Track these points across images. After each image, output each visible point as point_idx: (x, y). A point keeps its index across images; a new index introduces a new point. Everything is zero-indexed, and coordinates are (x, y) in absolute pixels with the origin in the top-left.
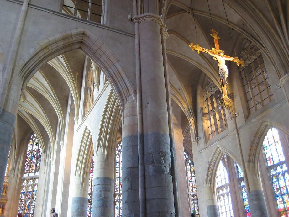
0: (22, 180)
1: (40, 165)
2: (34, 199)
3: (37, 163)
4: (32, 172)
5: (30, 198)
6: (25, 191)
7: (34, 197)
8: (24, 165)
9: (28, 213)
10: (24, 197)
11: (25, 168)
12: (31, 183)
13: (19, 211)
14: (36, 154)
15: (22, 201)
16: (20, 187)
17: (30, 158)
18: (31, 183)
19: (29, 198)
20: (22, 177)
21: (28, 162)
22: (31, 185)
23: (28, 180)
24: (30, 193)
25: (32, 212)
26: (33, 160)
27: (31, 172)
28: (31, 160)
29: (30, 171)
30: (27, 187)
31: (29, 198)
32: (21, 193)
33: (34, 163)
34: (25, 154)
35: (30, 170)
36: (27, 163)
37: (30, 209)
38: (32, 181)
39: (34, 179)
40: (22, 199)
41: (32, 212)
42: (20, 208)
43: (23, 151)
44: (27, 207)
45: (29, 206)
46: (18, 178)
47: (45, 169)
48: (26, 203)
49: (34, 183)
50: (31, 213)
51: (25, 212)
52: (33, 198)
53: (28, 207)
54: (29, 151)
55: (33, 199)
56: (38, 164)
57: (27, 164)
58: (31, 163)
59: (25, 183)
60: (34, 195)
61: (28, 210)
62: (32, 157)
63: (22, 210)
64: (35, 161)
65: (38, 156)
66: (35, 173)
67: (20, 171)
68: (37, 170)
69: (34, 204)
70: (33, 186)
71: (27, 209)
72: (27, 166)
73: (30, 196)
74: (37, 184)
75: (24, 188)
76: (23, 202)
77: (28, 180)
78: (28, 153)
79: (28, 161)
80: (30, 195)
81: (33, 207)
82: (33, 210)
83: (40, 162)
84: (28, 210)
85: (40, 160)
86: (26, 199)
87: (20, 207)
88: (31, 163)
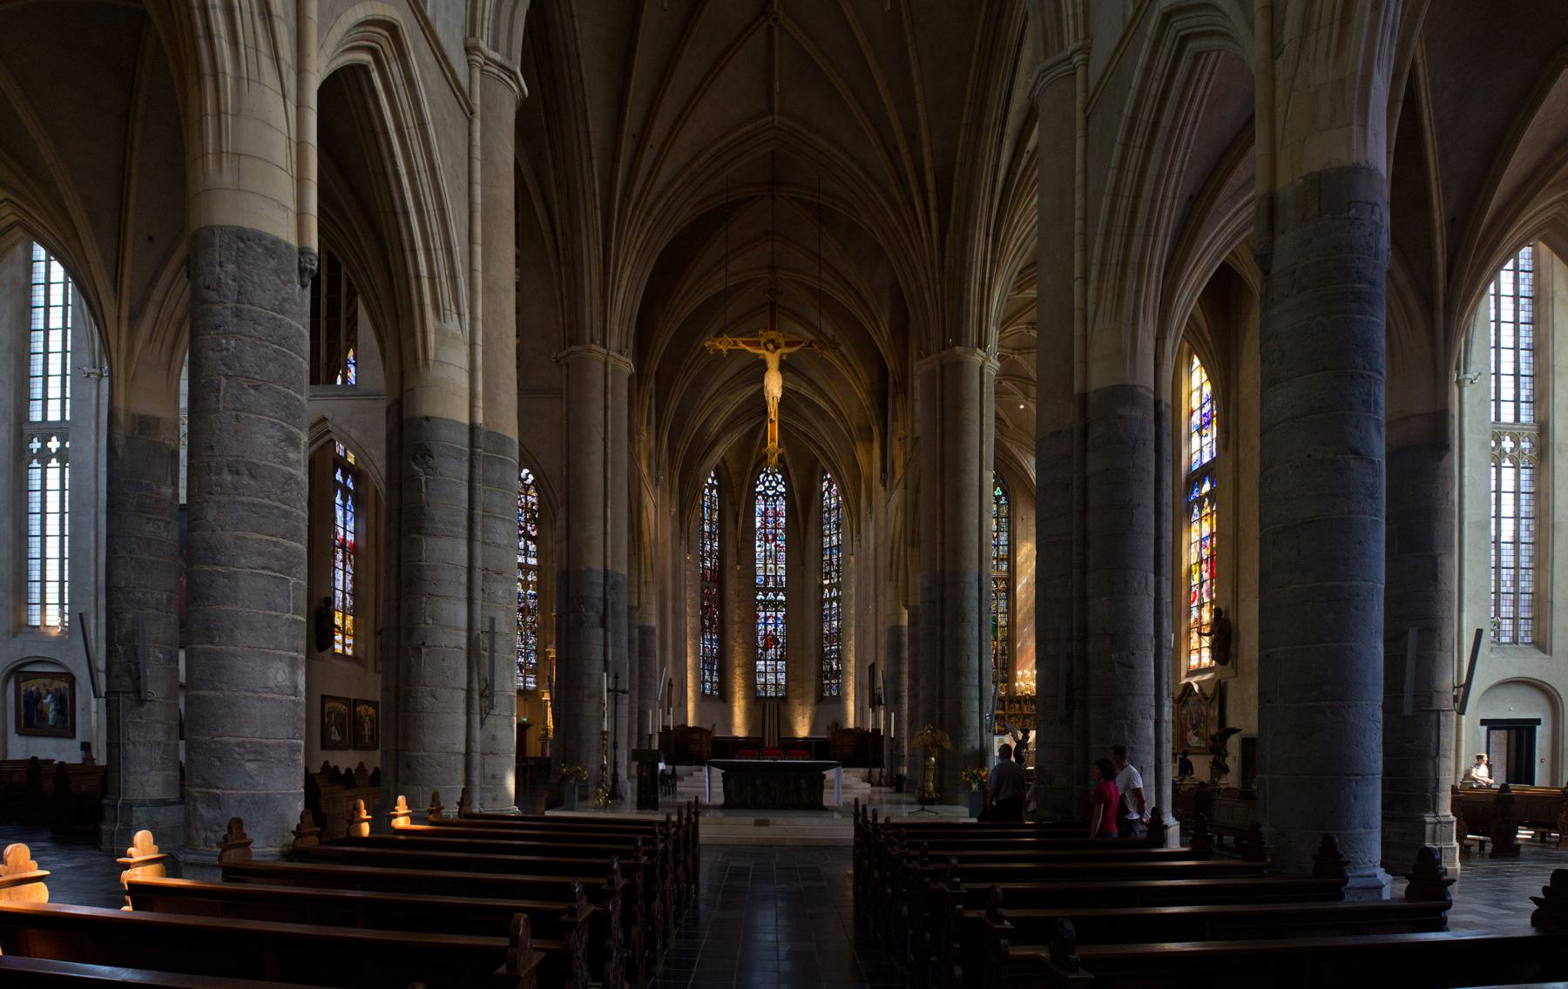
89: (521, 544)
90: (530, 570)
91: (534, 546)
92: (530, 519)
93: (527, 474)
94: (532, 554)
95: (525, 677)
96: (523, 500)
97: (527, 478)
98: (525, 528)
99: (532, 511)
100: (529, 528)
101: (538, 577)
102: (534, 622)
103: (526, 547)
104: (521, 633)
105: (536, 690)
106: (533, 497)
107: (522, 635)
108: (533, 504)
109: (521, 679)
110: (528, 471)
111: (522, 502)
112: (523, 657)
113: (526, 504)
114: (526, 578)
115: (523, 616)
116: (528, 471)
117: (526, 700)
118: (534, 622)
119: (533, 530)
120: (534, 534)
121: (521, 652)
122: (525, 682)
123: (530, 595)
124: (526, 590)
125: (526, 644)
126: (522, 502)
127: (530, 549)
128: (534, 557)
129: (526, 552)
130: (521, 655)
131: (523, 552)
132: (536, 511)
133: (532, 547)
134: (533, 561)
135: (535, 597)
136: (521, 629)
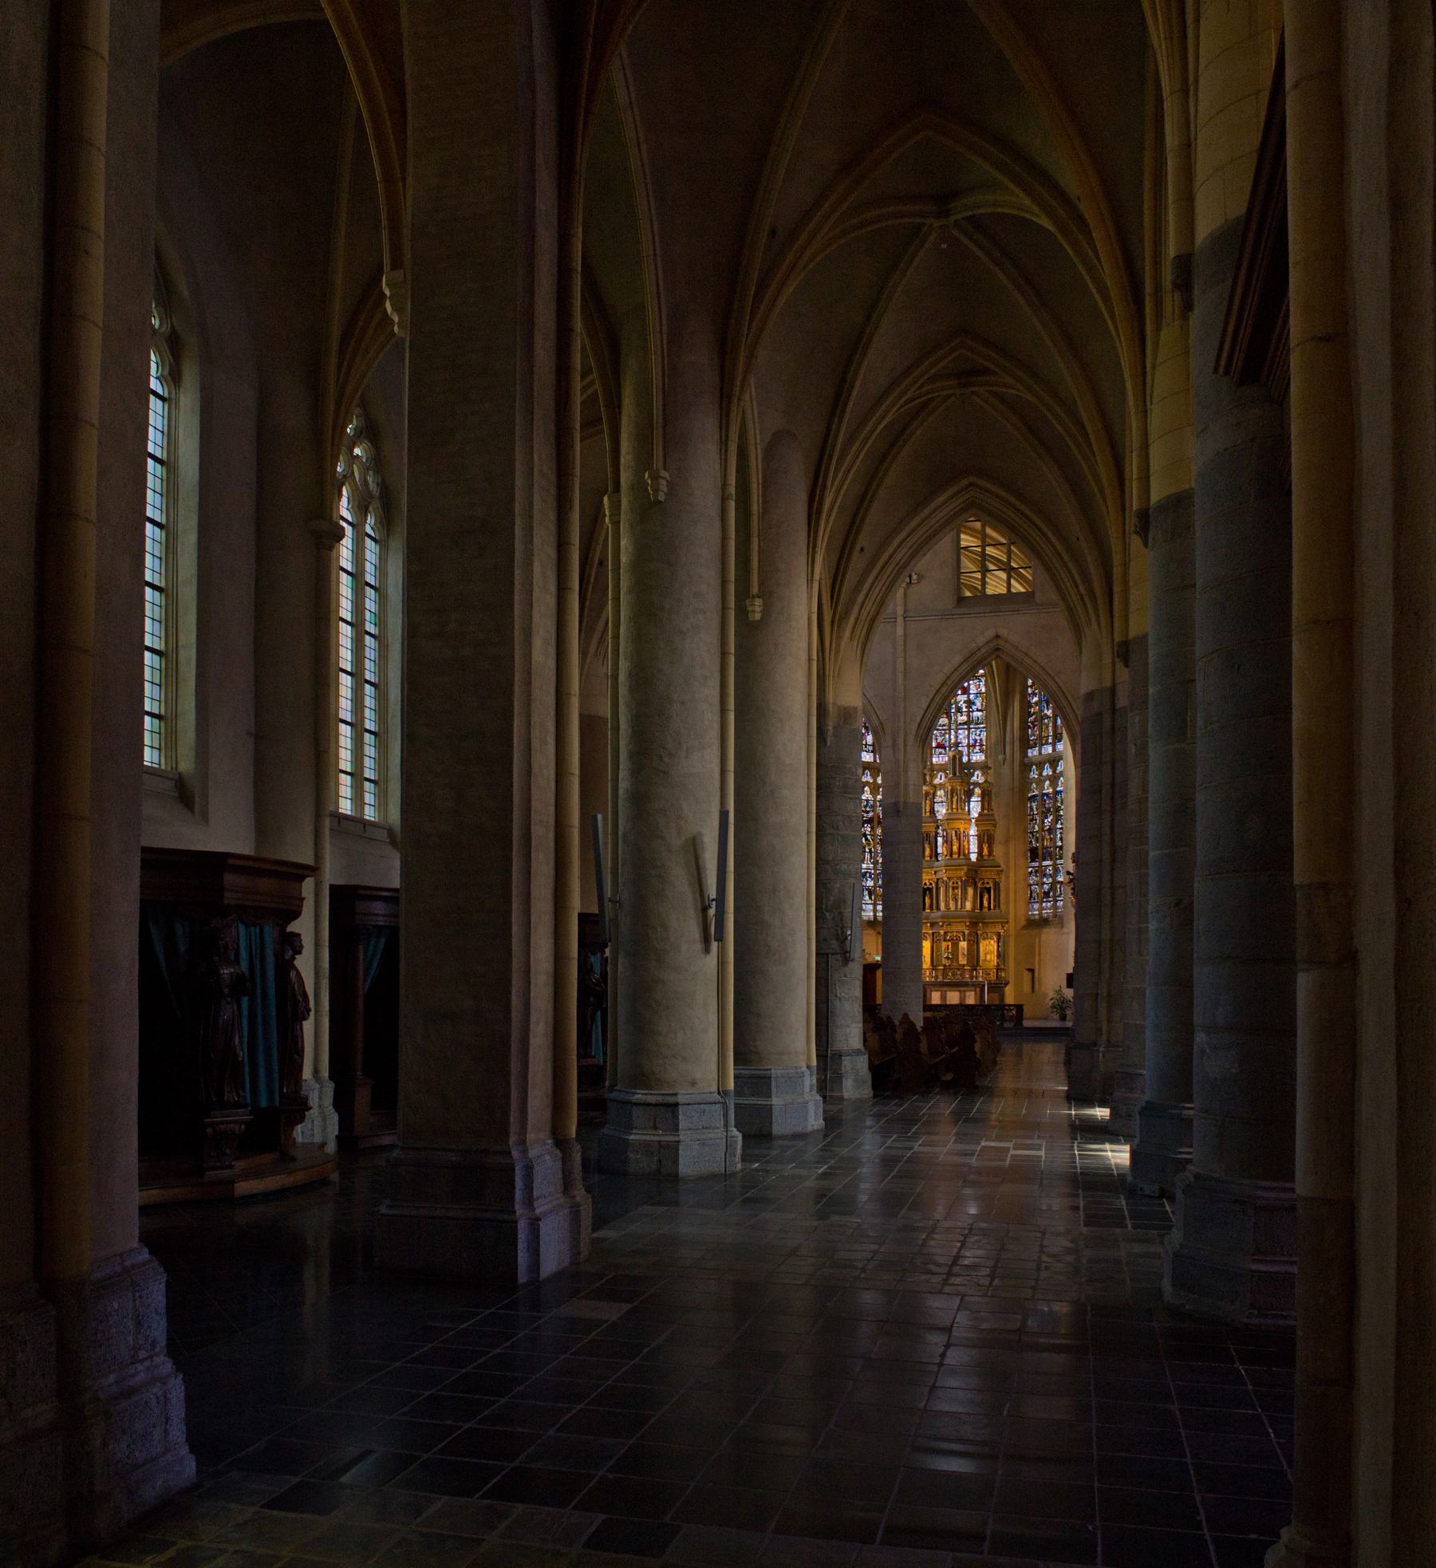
0: (1026, 766)
4: (1047, 743)
6: (1036, 793)
8: (1024, 726)
12: (1047, 771)
13: (1031, 842)
17: (1036, 703)
20: (1026, 759)
22: (1048, 777)
24: (1050, 798)
26: (1046, 712)
28: (1041, 711)
29: (1041, 742)
30: (1040, 783)
33: (1048, 717)
35: (1040, 737)
40: (1034, 814)
41: (1059, 844)
44: (1047, 833)
45: (1051, 830)
48: (1043, 821)
49: (1054, 771)
55: (1059, 811)
57: (1032, 723)
58: (1042, 719)
59: (1034, 775)
61: (1051, 839)
63: (1037, 841)
64: (1049, 713)
67: (1017, 744)
76: (1036, 820)
77: (1040, 766)
78: (1030, 691)
79: (1034, 713)
95: (875, 905)
107: (870, 852)
115: (872, 828)
121: (870, 873)
122: (875, 911)
124: (875, 797)
130: (870, 877)
136: (869, 845)
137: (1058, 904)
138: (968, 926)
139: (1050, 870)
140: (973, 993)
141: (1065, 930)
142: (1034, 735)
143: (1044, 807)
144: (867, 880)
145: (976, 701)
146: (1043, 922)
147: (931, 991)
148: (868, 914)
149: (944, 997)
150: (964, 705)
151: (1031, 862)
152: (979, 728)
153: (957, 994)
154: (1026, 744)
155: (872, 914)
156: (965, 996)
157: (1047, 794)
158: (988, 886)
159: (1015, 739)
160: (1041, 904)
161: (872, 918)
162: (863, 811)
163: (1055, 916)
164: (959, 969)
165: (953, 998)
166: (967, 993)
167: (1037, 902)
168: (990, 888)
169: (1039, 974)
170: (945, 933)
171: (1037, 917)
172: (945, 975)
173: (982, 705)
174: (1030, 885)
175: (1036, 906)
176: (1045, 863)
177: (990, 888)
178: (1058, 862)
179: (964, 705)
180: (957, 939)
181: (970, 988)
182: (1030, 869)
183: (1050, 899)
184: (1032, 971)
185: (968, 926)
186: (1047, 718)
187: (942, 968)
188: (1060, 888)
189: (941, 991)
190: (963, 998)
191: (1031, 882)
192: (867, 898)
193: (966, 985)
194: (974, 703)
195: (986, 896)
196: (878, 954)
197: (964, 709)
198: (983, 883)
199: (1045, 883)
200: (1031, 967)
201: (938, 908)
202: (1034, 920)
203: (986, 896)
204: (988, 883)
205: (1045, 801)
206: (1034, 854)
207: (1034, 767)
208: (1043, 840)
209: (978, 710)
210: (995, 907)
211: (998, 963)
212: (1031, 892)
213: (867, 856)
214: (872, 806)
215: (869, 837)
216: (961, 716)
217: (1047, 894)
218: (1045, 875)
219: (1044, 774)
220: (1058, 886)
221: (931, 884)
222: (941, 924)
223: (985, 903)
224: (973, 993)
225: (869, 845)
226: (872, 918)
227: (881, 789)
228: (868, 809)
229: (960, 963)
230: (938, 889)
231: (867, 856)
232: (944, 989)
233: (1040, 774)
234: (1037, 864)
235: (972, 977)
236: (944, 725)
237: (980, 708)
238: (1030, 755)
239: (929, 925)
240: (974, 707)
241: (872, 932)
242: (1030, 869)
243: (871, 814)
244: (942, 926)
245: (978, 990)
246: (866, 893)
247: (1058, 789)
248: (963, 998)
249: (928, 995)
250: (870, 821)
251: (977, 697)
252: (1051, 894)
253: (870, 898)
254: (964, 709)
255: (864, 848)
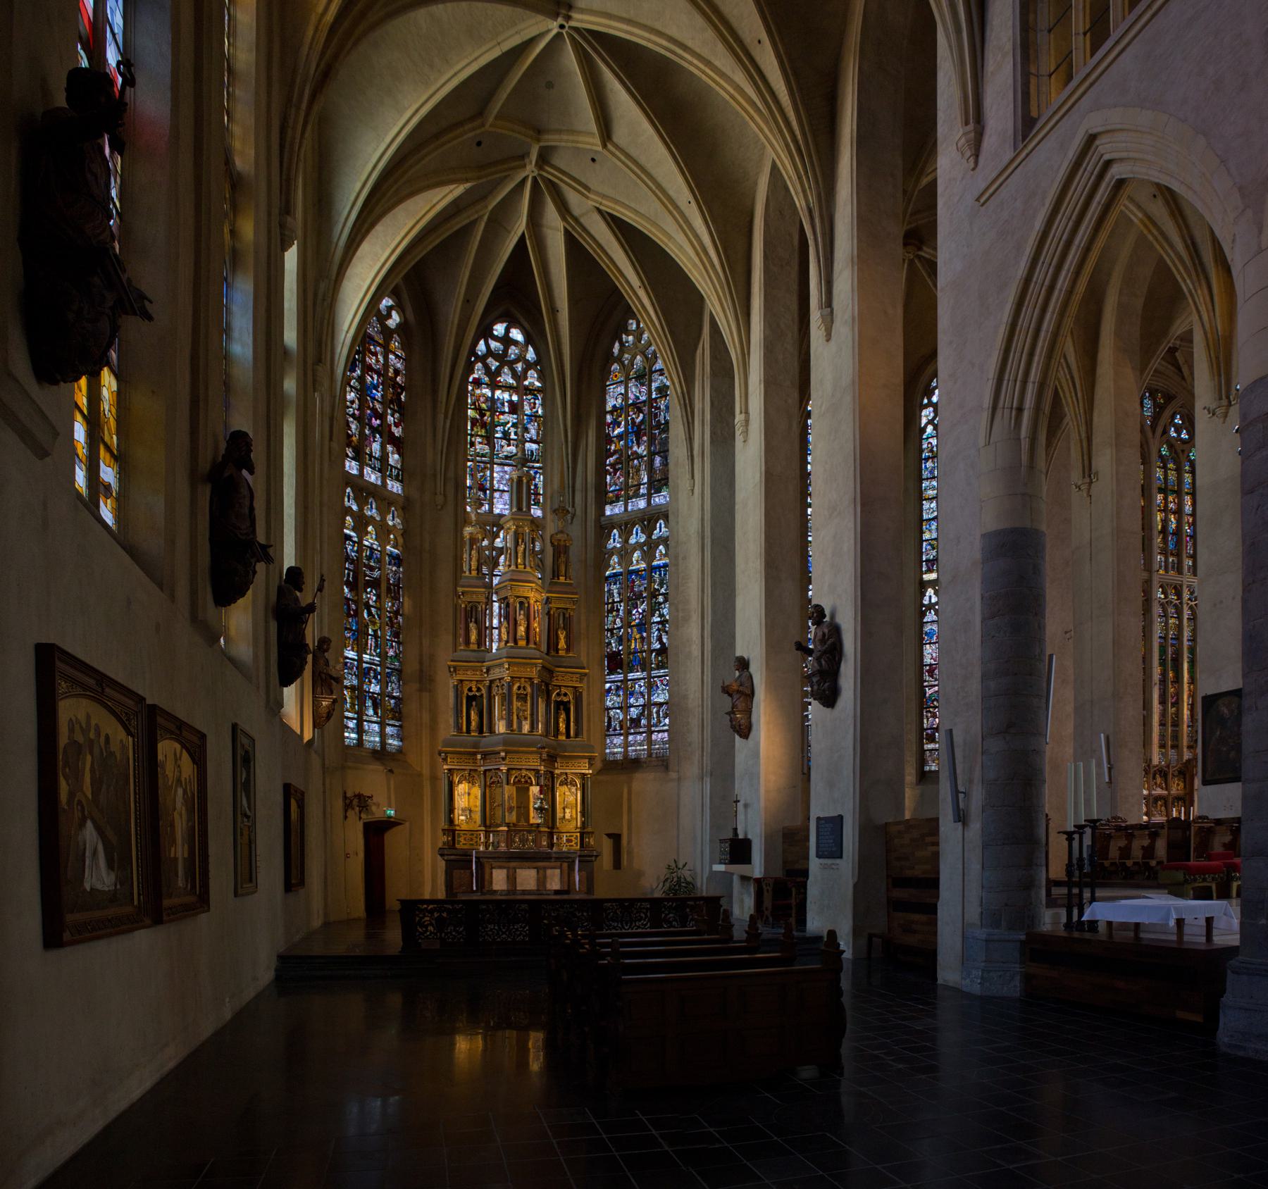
0: (604, 528)
1: (665, 463)
2: (661, 599)
3: (652, 455)
4: (637, 495)
5: (644, 595)
6: (618, 569)
7: (658, 590)
8: (601, 472)
9: (642, 652)
10: (619, 594)
11: (608, 480)
12: (638, 537)
13: (610, 644)
14: (642, 422)
15: (613, 607)
16: (602, 557)
17: (620, 437)
18: (638, 537)
19: (639, 596)
20: (603, 519)
21: (614, 457)
22: (639, 546)
23: (626, 527)
24: (642, 578)
25: (657, 646)
26: (635, 448)
27: (631, 493)
28: (627, 447)
29: (629, 492)
30: (625, 554)
31: (639, 596)
32: (607, 578)
33: (639, 457)
34: (601, 424)
35: (626, 486)
36: (612, 459)
37: (649, 636)
38: (643, 532)
39: (649, 520)
40: (614, 602)
41: (657, 646)
42: (612, 634)
43: (594, 412)
44: (635, 630)
45: (643, 626)
46: (589, 524)
47: (693, 477)
48: (629, 613)
49: (649, 536)
50: (654, 650)
51: (633, 646)
52: (654, 594)
53: (640, 632)
54: (611, 412)
55: (656, 597)
56: (658, 460)
57: (612, 465)
58: (629, 459)
59: (615, 542)
60: (655, 582)
61: (642, 638)
62: (626, 432)
63: (620, 640)
64: (642, 450)
65: (651, 428)
66: (649, 496)
67: (591, 494)
68: (660, 482)
69: (661, 615)
70: (649, 549)
71: (638, 636)
72: (616, 471)
73: (642, 588)
74: (664, 541)
75: (615, 559)
76: (618, 610)
77: (626, 527)
78: (609, 418)
79: (615, 452)
80: (640, 585)
81: (658, 630)
82: (660, 639)
83: (664, 453)
84: (642, 638)
85: (665, 442)
86: (629, 599)
87: (611, 630)
88: (626, 460)
89: (376, 447)
90: (390, 504)
91: (396, 456)
92: (391, 402)
93: (390, 309)
94: (395, 472)
95: (382, 725)
96: (381, 358)
97: (389, 316)
98: (382, 417)
99: (395, 385)
100: (390, 419)
101: (405, 521)
102: (397, 613)
103: (384, 458)
104: (375, 631)
105: (400, 750)
106: (397, 356)
107: (375, 636)
108: (397, 372)
109: (376, 727)
110: (390, 303)
111: (377, 361)
112: (379, 682)
113: (386, 364)
114: (384, 519)
115: (378, 596)
116: (390, 303)
117: (391, 771)
118: (397, 613)
119: (396, 425)
120: (397, 432)
121: (375, 670)
122: (382, 734)
123: (391, 555)
124: (383, 545)
125: (383, 656)
126: (377, 361)
127: (391, 461)
128: (397, 479)
129: (383, 467)
130: (375, 678)
131: (378, 465)
132: (403, 389)
133: (394, 459)
134: (394, 487)
135: (397, 560)
136: (374, 623)
137: (654, 737)
138: (544, 760)
139: (641, 687)
140: (558, 871)
141: (673, 775)
142: (616, 485)
143: (632, 590)
144: (370, 682)
145: (529, 426)
146: (631, 765)
147: (492, 868)
148: (372, 739)
149: (512, 879)
150: (512, 430)
151: (608, 674)
152: (533, 467)
153: (533, 873)
154: (603, 498)
155: (377, 739)
156: (545, 876)
157: (637, 572)
158: (565, 699)
159: (589, 485)
160: (626, 738)
161: (378, 747)
162: (365, 566)
163: (650, 755)
164: (529, 832)
165: (527, 878)
166: (549, 872)
167: (621, 735)
168: (569, 702)
169: (629, 842)
170: (509, 770)
171: (619, 757)
172: (509, 842)
173: (538, 433)
174: (609, 709)
175: (618, 740)
176: (631, 676)
177: (569, 702)
178: (654, 673)
179: (512, 430)
180: (526, 782)
181: (552, 864)
182: (608, 686)
183: (641, 730)
184: (616, 838)
185: (544, 760)
186: (638, 459)
187: (506, 829)
188: (658, 712)
189: (508, 868)
190: (542, 881)
191: (609, 704)
192: (371, 712)
193: (547, 857)
194: (526, 430)
195: (563, 717)
196: (390, 806)
197: (513, 436)
198: (558, 694)
199: (632, 706)
200: (616, 832)
201: (491, 730)
202: (615, 762)
203: (563, 717)
204: (565, 695)
205: (633, 582)
206: (615, 662)
207: (615, 531)
208: (629, 640)
209: (532, 441)
210: (577, 735)
211: (583, 823)
212: (610, 718)
213: (371, 641)
214: (379, 561)
215: (373, 610)
216: (509, 445)
217: (636, 722)
218: (632, 694)
219: (632, 540)
220: (655, 710)
221: (479, 690)
222: (503, 754)
223: (562, 726)
224: (558, 871)
225: (374, 623)
226: (378, 747)
227: (392, 536)
228: (372, 564)
229: (532, 821)
230: (491, 698)
231: (371, 641)
232: (513, 864)
233: (626, 541)
234: (621, 677)
235: (551, 845)
236: (483, 456)
237: (535, 438)
238: (608, 513)
239: (479, 757)
240: (527, 436)
241: (381, 768)
242: (608, 686)
243: (376, 574)
244: (504, 759)
245: (565, 865)
246: (369, 703)
247: (655, 563)
248: (542, 881)
249: (487, 877)
250: (375, 584)
251: (531, 421)
252: (643, 722)
253: (376, 713)
254: (513, 436)
255: (367, 627)
